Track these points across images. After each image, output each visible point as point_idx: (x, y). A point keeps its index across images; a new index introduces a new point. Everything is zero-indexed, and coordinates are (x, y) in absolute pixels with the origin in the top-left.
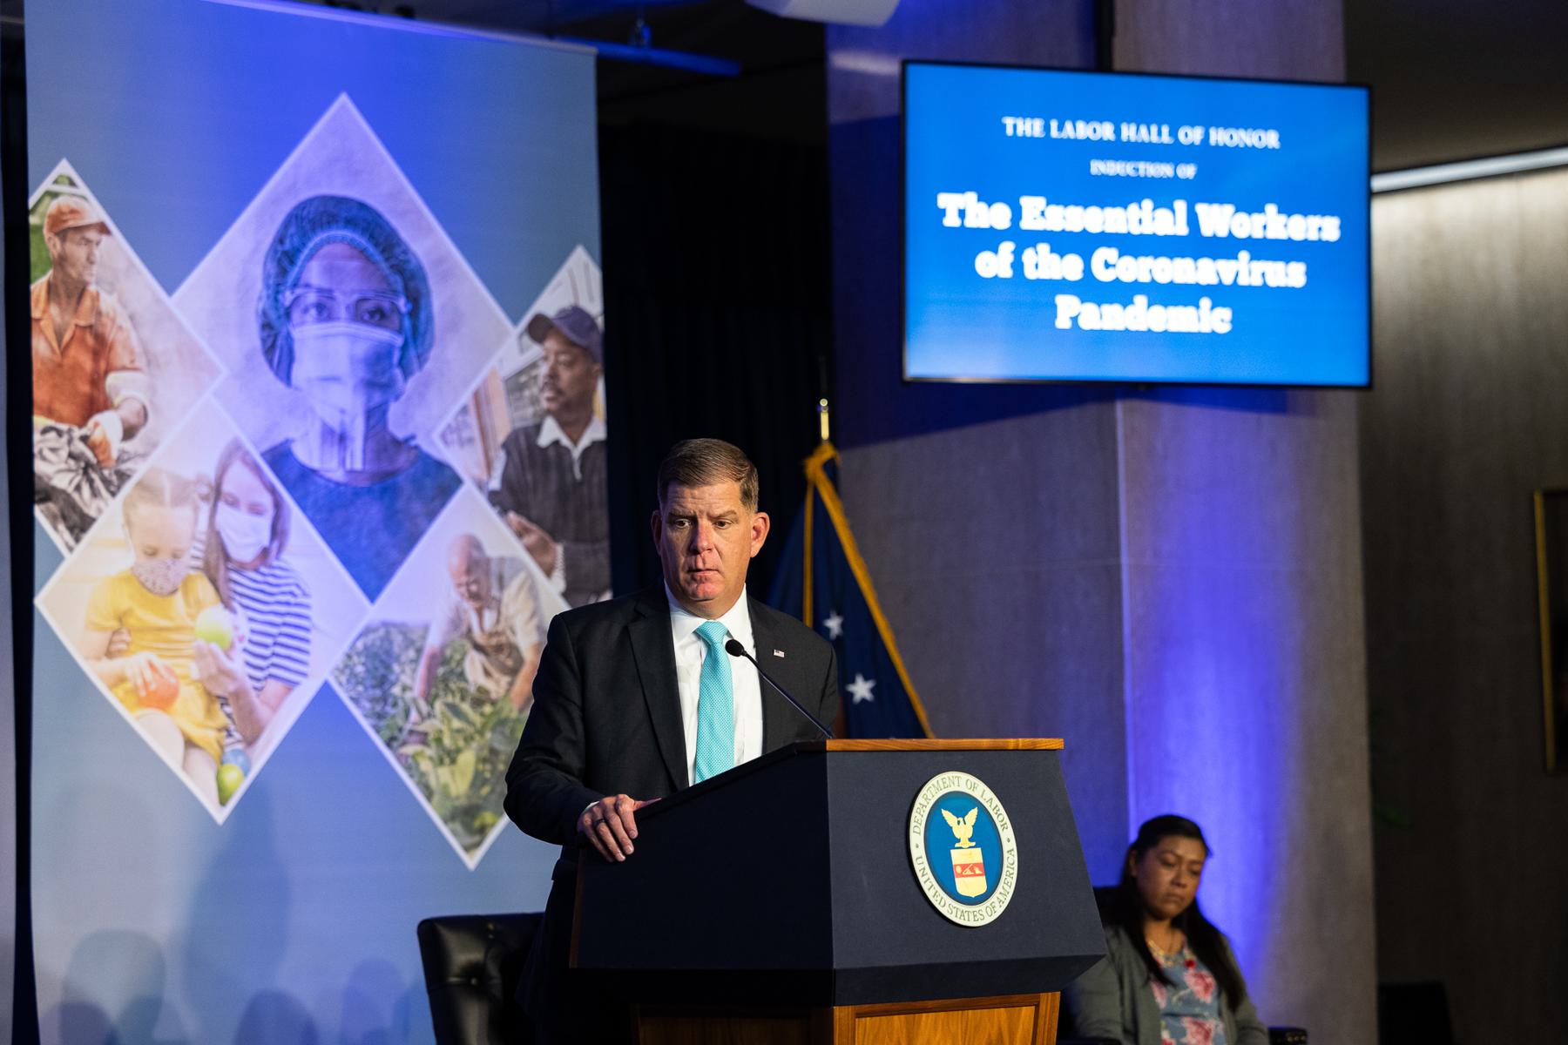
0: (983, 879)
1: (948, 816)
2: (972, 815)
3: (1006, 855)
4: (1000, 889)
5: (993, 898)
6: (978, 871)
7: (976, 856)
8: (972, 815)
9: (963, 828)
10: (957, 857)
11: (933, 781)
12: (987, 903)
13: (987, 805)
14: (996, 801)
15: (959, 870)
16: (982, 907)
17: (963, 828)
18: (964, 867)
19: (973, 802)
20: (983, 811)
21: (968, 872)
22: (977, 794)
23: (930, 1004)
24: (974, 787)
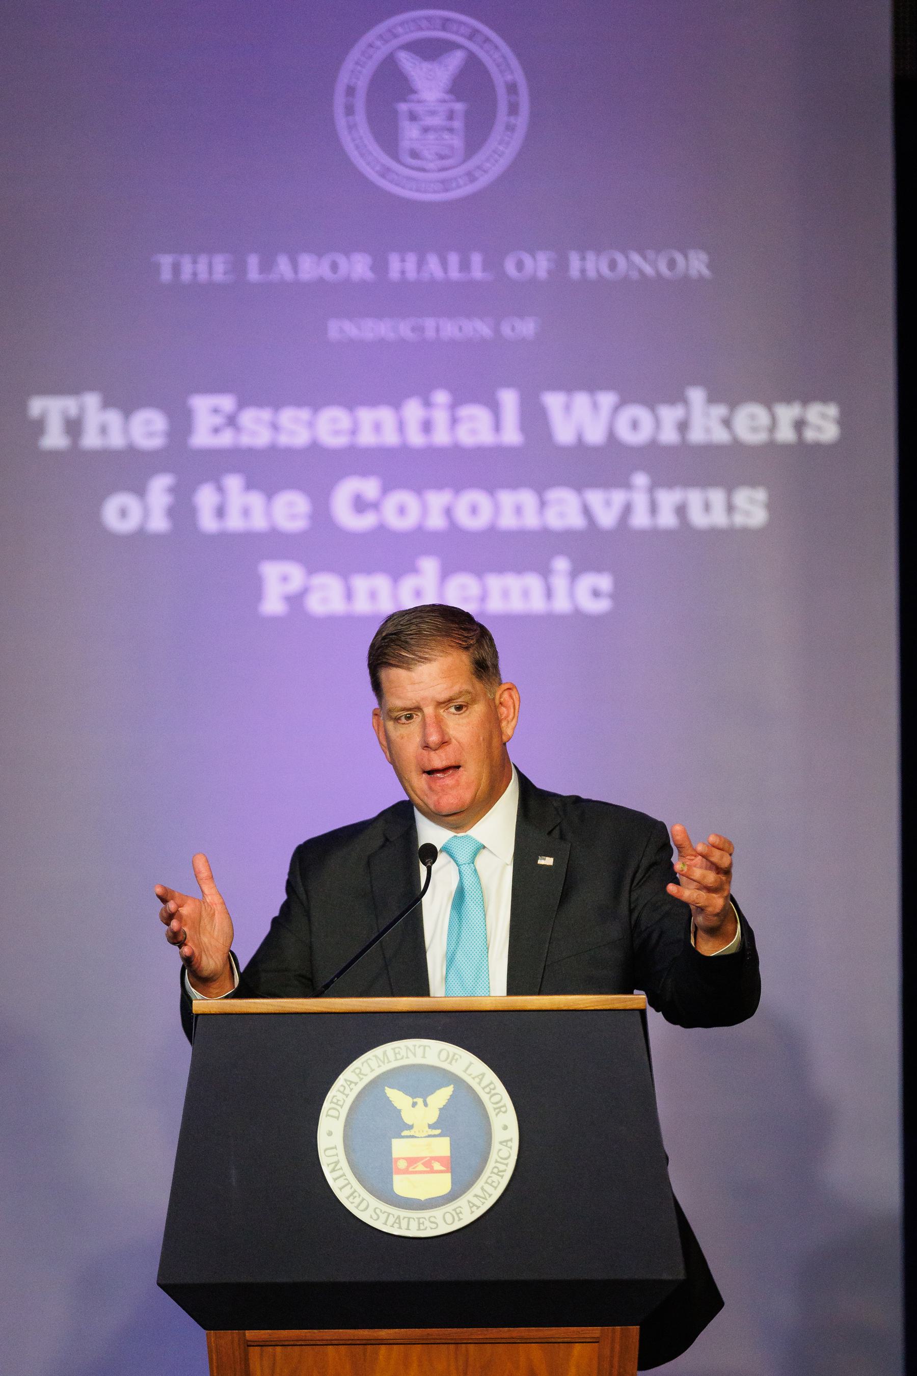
0: (447, 1177)
1: (397, 1097)
2: (442, 1096)
3: (495, 1146)
4: (476, 1189)
5: (462, 1202)
6: (437, 1166)
7: (442, 1147)
8: (442, 1096)
9: (420, 1113)
10: (400, 1148)
11: (378, 1051)
12: (450, 1207)
13: (474, 1084)
14: (491, 1076)
15: (402, 1165)
16: (437, 1213)
17: (420, 1113)
18: (412, 1161)
19: (445, 1077)
20: (465, 1092)
21: (420, 1167)
22: (457, 1068)
23: (384, 1333)
24: (452, 1059)
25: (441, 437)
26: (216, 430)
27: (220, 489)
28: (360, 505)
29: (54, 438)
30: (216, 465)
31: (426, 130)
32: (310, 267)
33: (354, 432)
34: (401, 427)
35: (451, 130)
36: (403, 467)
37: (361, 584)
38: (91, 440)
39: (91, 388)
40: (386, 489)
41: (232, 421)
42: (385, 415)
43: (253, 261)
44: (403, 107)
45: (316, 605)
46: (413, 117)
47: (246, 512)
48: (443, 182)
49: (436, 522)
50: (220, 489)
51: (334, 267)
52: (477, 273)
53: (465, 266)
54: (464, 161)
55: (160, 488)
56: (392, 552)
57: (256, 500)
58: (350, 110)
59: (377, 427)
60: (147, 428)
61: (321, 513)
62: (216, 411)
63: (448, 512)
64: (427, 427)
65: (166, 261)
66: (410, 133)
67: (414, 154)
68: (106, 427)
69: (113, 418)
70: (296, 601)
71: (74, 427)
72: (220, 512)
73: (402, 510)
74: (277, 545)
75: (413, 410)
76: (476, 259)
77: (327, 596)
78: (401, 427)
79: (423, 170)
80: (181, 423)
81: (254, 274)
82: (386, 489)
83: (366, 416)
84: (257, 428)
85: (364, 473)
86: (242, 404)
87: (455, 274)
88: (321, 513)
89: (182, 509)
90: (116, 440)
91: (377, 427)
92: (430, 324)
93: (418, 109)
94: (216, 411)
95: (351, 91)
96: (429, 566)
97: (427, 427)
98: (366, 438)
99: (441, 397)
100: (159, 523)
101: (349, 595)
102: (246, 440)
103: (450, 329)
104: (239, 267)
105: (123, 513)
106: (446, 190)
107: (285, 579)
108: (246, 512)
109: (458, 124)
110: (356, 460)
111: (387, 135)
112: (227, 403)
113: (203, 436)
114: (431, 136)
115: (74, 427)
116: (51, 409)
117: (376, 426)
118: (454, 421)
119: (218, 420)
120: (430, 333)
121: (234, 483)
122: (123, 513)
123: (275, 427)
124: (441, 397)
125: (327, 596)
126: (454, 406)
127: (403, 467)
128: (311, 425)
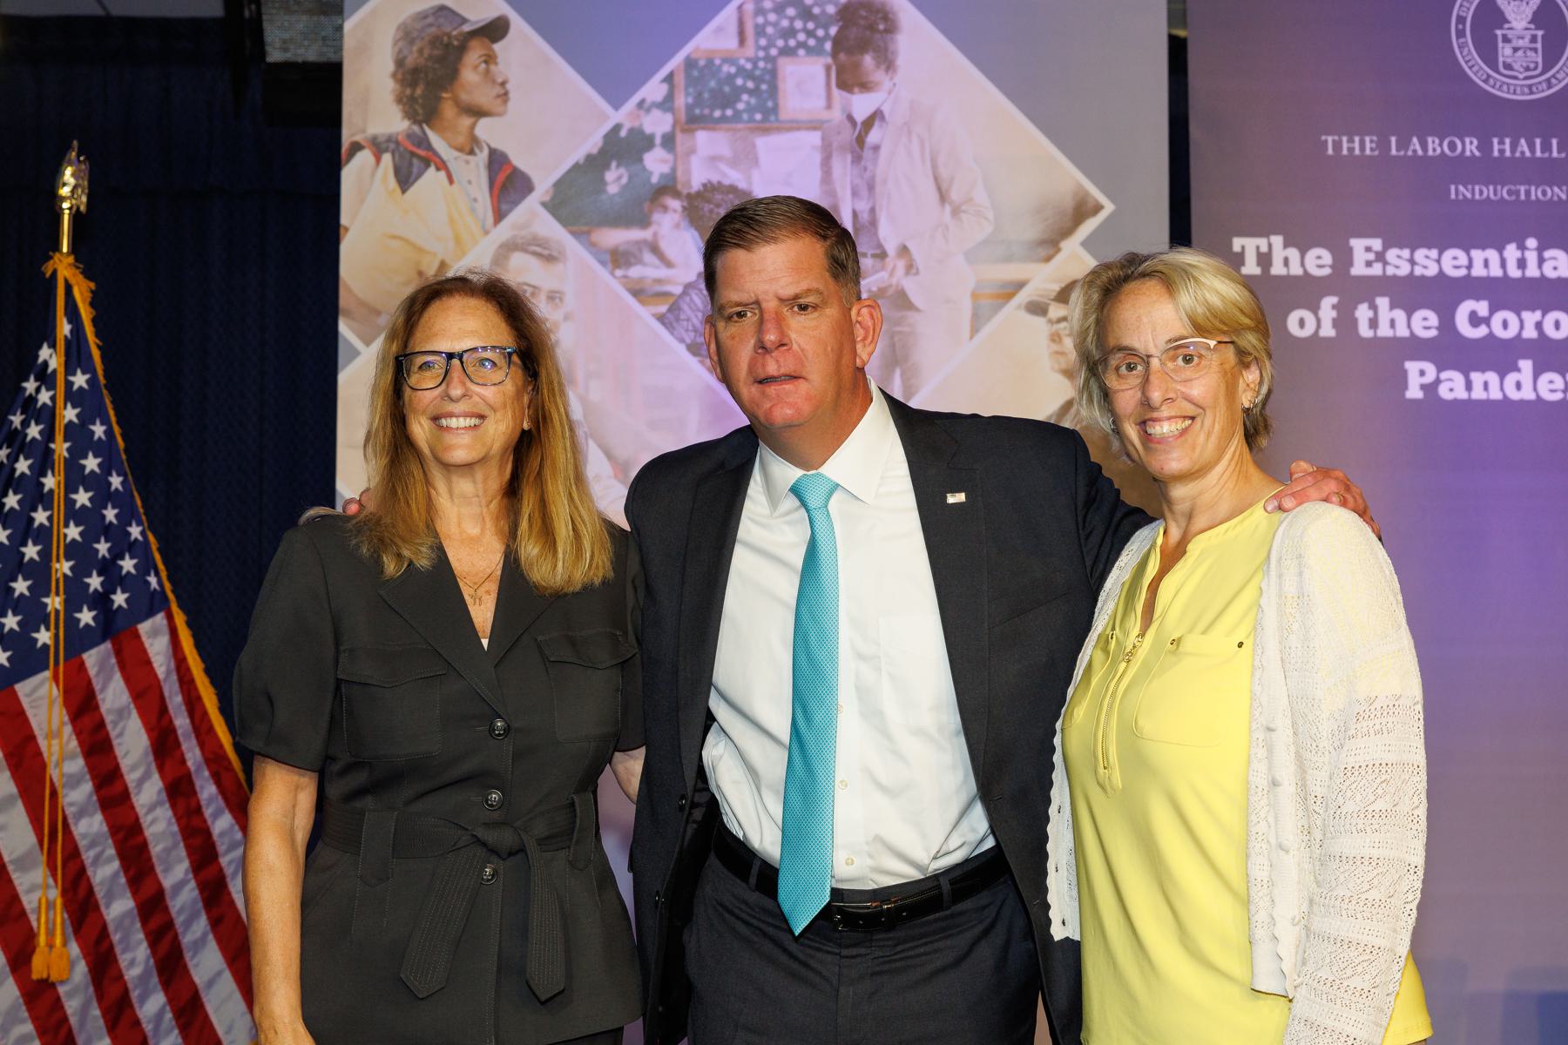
25: (1532, 271)
26: (1369, 264)
27: (1374, 307)
28: (1475, 320)
29: (1251, 268)
30: (1369, 289)
31: (1516, 50)
32: (1434, 146)
33: (1469, 267)
34: (1503, 264)
35: (1535, 50)
36: (1505, 293)
37: (1477, 378)
38: (1277, 269)
39: (1276, 233)
40: (1493, 309)
41: (1380, 257)
42: (1492, 255)
43: (1393, 139)
44: (1499, 32)
45: (1444, 392)
46: (1506, 39)
47: (1392, 323)
48: (1530, 87)
49: (1530, 333)
50: (1374, 307)
51: (1452, 146)
52: (1555, 154)
53: (1546, 147)
54: (1545, 70)
55: (1328, 304)
56: (1500, 356)
57: (1399, 315)
58: (1461, 34)
59: (1486, 263)
60: (1319, 261)
61: (1447, 324)
62: (1368, 249)
63: (1539, 326)
64: (1522, 264)
65: (1330, 139)
66: (1505, 51)
67: (1508, 67)
68: (1287, 260)
69: (1293, 253)
70: (1430, 389)
71: (1265, 259)
72: (1374, 323)
73: (1505, 325)
74: (1415, 348)
75: (1512, 252)
76: (1554, 142)
77: (1453, 386)
78: (1503, 264)
79: (1515, 78)
80: (1343, 258)
81: (1394, 152)
82: (1493, 309)
83: (1478, 255)
84: (1398, 262)
85: (1478, 299)
86: (1386, 247)
87: (1538, 154)
88: (1447, 324)
89: (1345, 321)
90: (1296, 270)
91: (1486, 263)
92: (1522, 189)
93: (1510, 34)
94: (1368, 249)
95: (1461, 20)
96: (1526, 365)
97: (1522, 264)
98: (1478, 271)
99: (1532, 243)
100: (1328, 331)
101: (1469, 386)
102: (1390, 271)
103: (1536, 193)
104: (1383, 145)
105: (1302, 323)
106: (1531, 93)
107: (1422, 373)
108: (1392, 323)
109: (1539, 45)
110: (1470, 287)
111: (1488, 52)
112: (1377, 244)
113: (1359, 269)
114: (1520, 53)
115: (1265, 259)
116: (1247, 245)
117: (1486, 262)
118: (1541, 261)
119: (1371, 256)
120: (1523, 197)
121: (1383, 302)
122: (1302, 323)
123: (1412, 262)
124: (1532, 243)
125: (1453, 386)
126: (1540, 250)
127: (1505, 293)
128: (1438, 261)
